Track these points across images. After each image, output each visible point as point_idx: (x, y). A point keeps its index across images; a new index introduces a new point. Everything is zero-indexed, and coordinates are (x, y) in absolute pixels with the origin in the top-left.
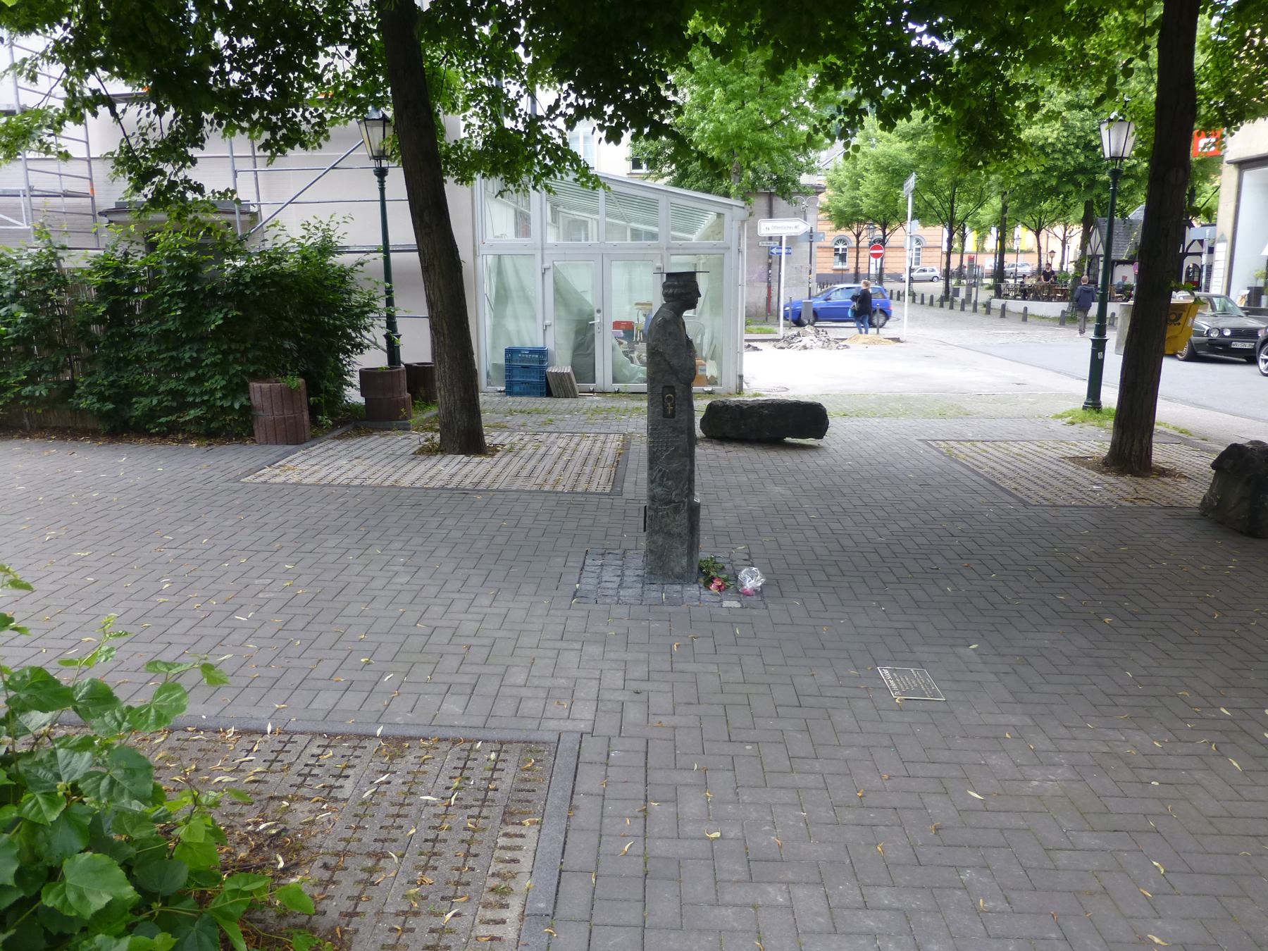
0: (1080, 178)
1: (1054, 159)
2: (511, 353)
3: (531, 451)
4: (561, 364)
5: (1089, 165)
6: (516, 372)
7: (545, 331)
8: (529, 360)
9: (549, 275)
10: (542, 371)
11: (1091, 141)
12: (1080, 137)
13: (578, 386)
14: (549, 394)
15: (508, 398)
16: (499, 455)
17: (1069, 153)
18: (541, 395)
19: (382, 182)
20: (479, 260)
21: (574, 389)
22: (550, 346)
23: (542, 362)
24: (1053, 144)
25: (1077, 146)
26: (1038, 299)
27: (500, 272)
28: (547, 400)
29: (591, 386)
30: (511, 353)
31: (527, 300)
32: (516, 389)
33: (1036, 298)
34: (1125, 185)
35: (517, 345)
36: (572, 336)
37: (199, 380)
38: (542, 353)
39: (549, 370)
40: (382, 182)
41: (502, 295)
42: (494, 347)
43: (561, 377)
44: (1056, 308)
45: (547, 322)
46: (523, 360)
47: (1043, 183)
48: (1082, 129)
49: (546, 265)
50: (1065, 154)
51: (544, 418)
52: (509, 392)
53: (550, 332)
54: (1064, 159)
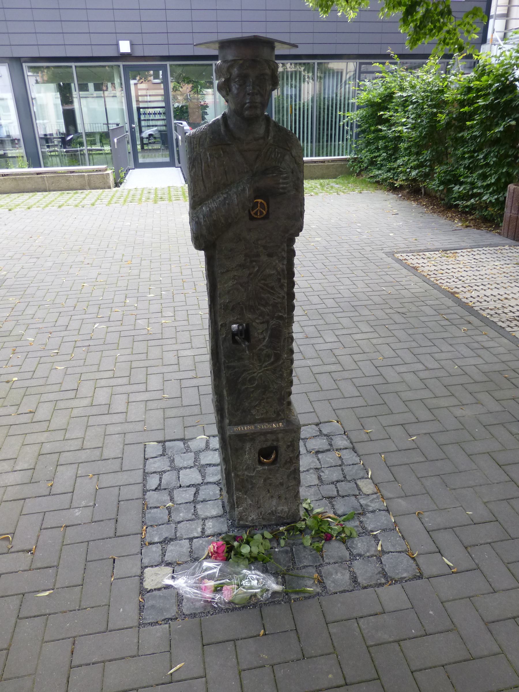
37: (484, 177)
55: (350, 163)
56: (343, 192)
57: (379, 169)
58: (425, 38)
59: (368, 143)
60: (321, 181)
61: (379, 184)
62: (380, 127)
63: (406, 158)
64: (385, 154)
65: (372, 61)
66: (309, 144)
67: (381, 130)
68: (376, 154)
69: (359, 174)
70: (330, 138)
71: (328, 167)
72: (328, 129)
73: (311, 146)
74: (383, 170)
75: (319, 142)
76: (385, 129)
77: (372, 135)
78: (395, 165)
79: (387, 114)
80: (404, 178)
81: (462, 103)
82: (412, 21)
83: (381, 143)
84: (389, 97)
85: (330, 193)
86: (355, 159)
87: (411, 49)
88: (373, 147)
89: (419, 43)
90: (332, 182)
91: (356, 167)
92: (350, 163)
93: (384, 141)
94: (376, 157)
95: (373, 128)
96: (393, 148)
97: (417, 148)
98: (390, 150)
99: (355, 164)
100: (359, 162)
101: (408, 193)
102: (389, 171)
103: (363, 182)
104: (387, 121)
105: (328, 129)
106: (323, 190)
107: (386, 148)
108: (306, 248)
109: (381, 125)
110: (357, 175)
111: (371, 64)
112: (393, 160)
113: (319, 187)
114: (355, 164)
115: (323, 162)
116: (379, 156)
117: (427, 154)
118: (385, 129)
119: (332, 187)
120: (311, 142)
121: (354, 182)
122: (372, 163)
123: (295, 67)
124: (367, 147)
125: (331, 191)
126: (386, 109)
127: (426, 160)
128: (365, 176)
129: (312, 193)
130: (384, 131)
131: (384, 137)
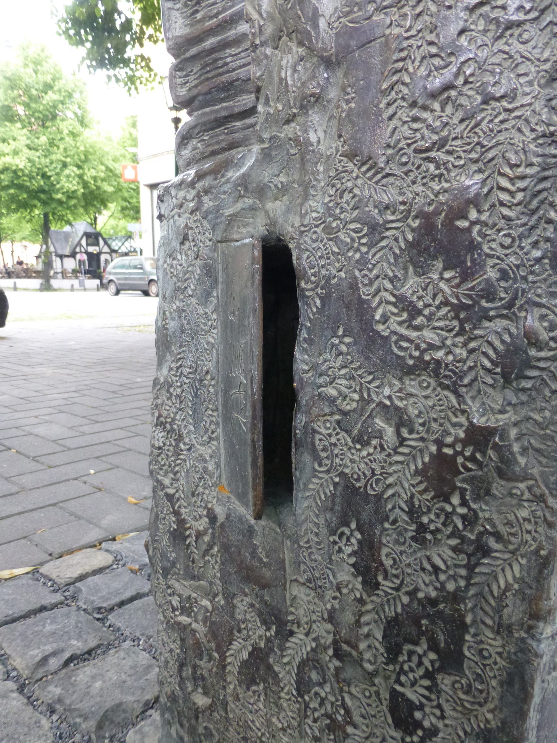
0: (42, 196)
1: (24, 180)
5: (46, 188)
11: (46, 173)
12: (39, 169)
17: (33, 178)
24: (21, 170)
25: (38, 175)
26: (20, 278)
33: (18, 277)
34: (73, 202)
44: (36, 283)
47: (18, 196)
48: (40, 164)
50: (30, 179)
54: (31, 182)
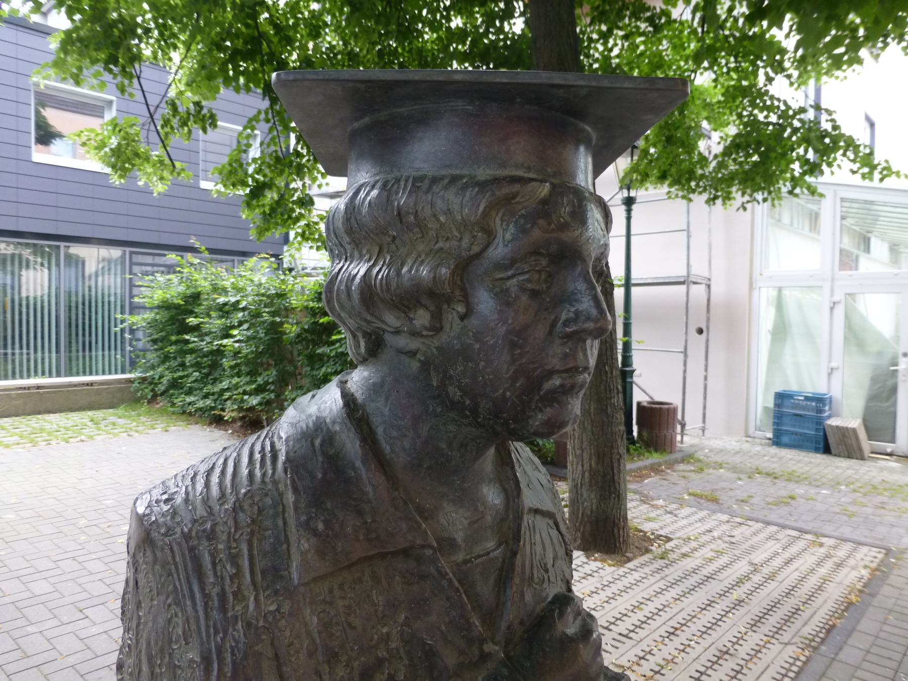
2: (782, 398)
3: (698, 562)
4: (848, 416)
6: (786, 420)
7: (830, 374)
8: (803, 408)
9: (840, 311)
10: (819, 423)
13: (866, 444)
14: (827, 450)
15: (774, 450)
16: (647, 557)
18: (817, 450)
19: (629, 211)
20: (755, 293)
21: (860, 449)
22: (836, 392)
23: (820, 411)
27: (780, 306)
28: (820, 458)
29: (889, 447)
30: (782, 398)
31: (810, 336)
32: (785, 439)
35: (794, 387)
36: (867, 383)
38: (820, 402)
39: (833, 422)
40: (629, 211)
41: (780, 331)
42: (767, 389)
43: (846, 434)
45: (834, 365)
46: (797, 406)
49: (836, 298)
51: (783, 489)
52: (777, 441)
53: (837, 376)
55: (136, 384)
56: (137, 431)
57: (189, 392)
58: (276, 229)
59: (166, 358)
60: (90, 413)
61: (188, 415)
62: (187, 337)
63: (235, 380)
64: (197, 374)
65: (166, 252)
66: (54, 355)
67: (187, 342)
68: (181, 374)
69: (152, 400)
70: (88, 347)
71: (98, 393)
72: (84, 335)
73: (57, 359)
74: (195, 396)
75: (70, 352)
76: (196, 339)
77: (174, 347)
78: (216, 389)
79: (192, 321)
80: (236, 407)
81: (313, 312)
82: (258, 206)
83: (189, 359)
84: (195, 298)
85: (115, 435)
86: (144, 379)
87: (258, 239)
88: (174, 363)
89: (268, 234)
90: (109, 415)
91: (146, 391)
92: (136, 384)
93: (194, 356)
94: (181, 377)
95: (173, 338)
96: (209, 366)
97: (253, 367)
98: (204, 368)
99: (144, 386)
100: (151, 383)
101: (242, 426)
102: (206, 396)
103: (163, 412)
104: (196, 328)
105: (84, 335)
106: (99, 429)
107: (198, 366)
108: (109, 553)
109: (186, 334)
110: (149, 402)
111: (165, 255)
112: (211, 382)
113: (90, 424)
114: (144, 386)
115: (91, 384)
116: (188, 376)
117: (269, 375)
118: (196, 339)
119: (114, 424)
120: (58, 352)
121: (149, 413)
122: (175, 384)
123: (16, 248)
124: (163, 362)
125: (116, 431)
126: (191, 313)
127: (267, 383)
128: (162, 403)
129: (83, 437)
130: (194, 342)
131: (192, 351)
